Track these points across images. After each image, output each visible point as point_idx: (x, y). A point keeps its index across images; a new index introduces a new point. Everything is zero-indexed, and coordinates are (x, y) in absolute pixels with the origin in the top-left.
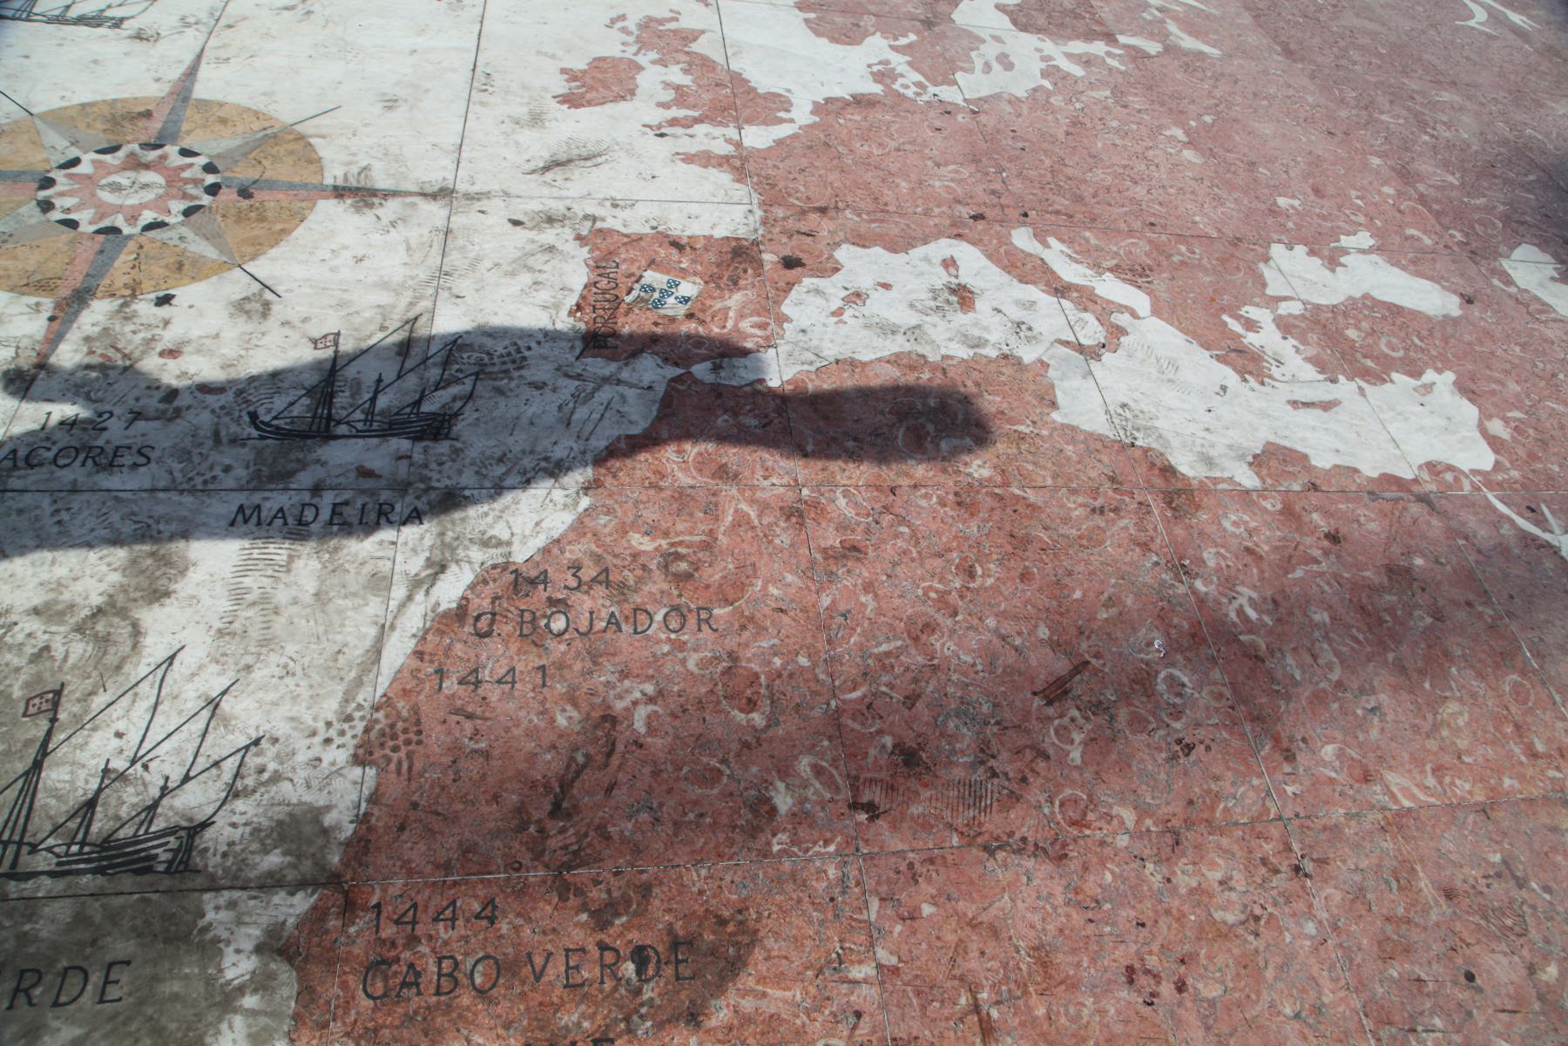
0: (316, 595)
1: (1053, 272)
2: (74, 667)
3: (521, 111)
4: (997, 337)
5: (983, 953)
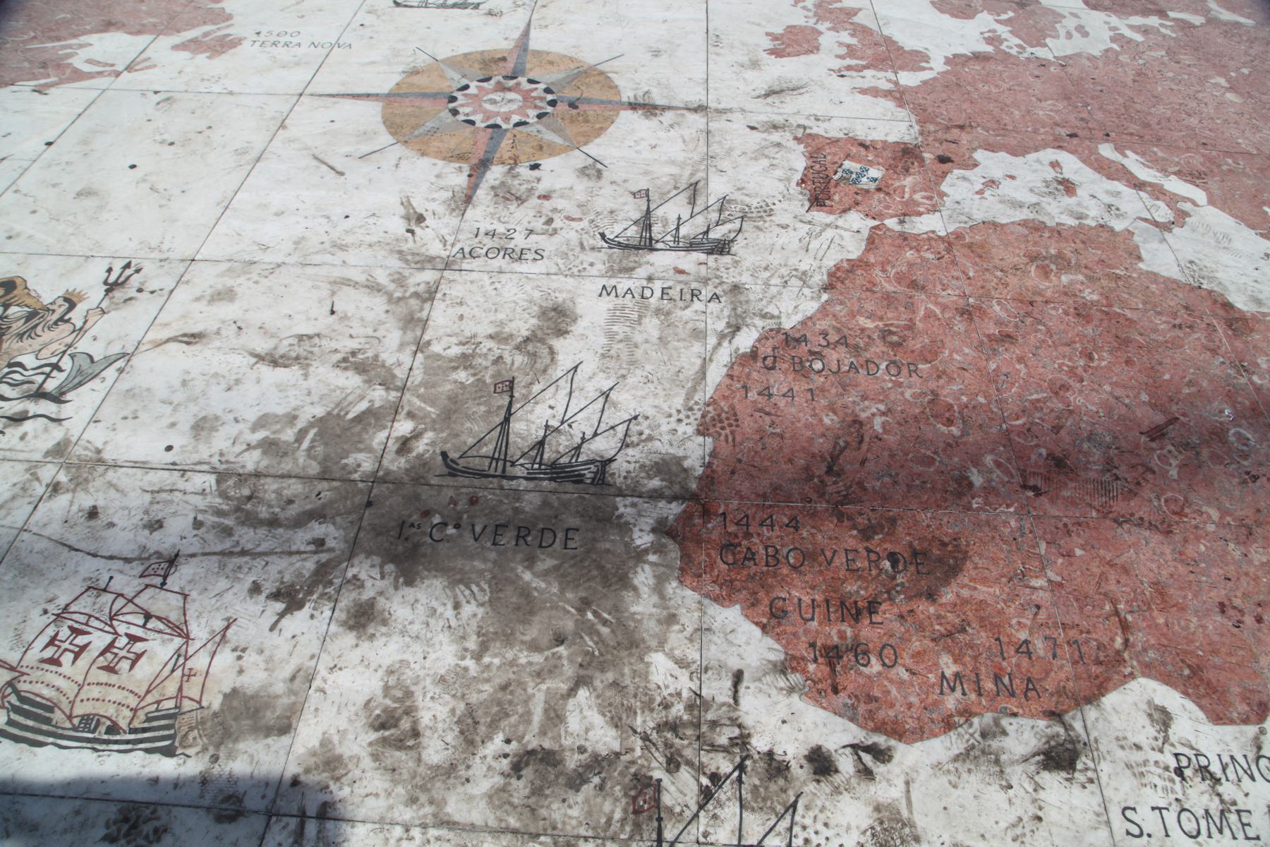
0: (660, 338)
1: (1131, 173)
2: (519, 369)
3: (745, 59)
4: (1094, 212)
5: (1118, 582)
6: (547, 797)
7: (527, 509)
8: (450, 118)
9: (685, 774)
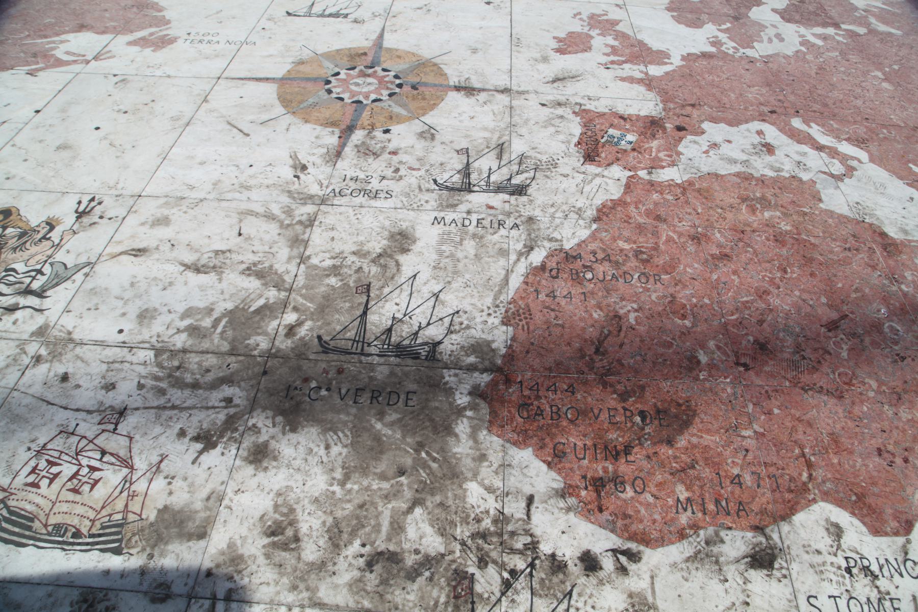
0: (476, 255)
1: (814, 139)
2: (374, 276)
3: (538, 56)
4: (788, 168)
5: (805, 433)
6: (391, 586)
7: (379, 377)
8: (326, 96)
9: (491, 570)
